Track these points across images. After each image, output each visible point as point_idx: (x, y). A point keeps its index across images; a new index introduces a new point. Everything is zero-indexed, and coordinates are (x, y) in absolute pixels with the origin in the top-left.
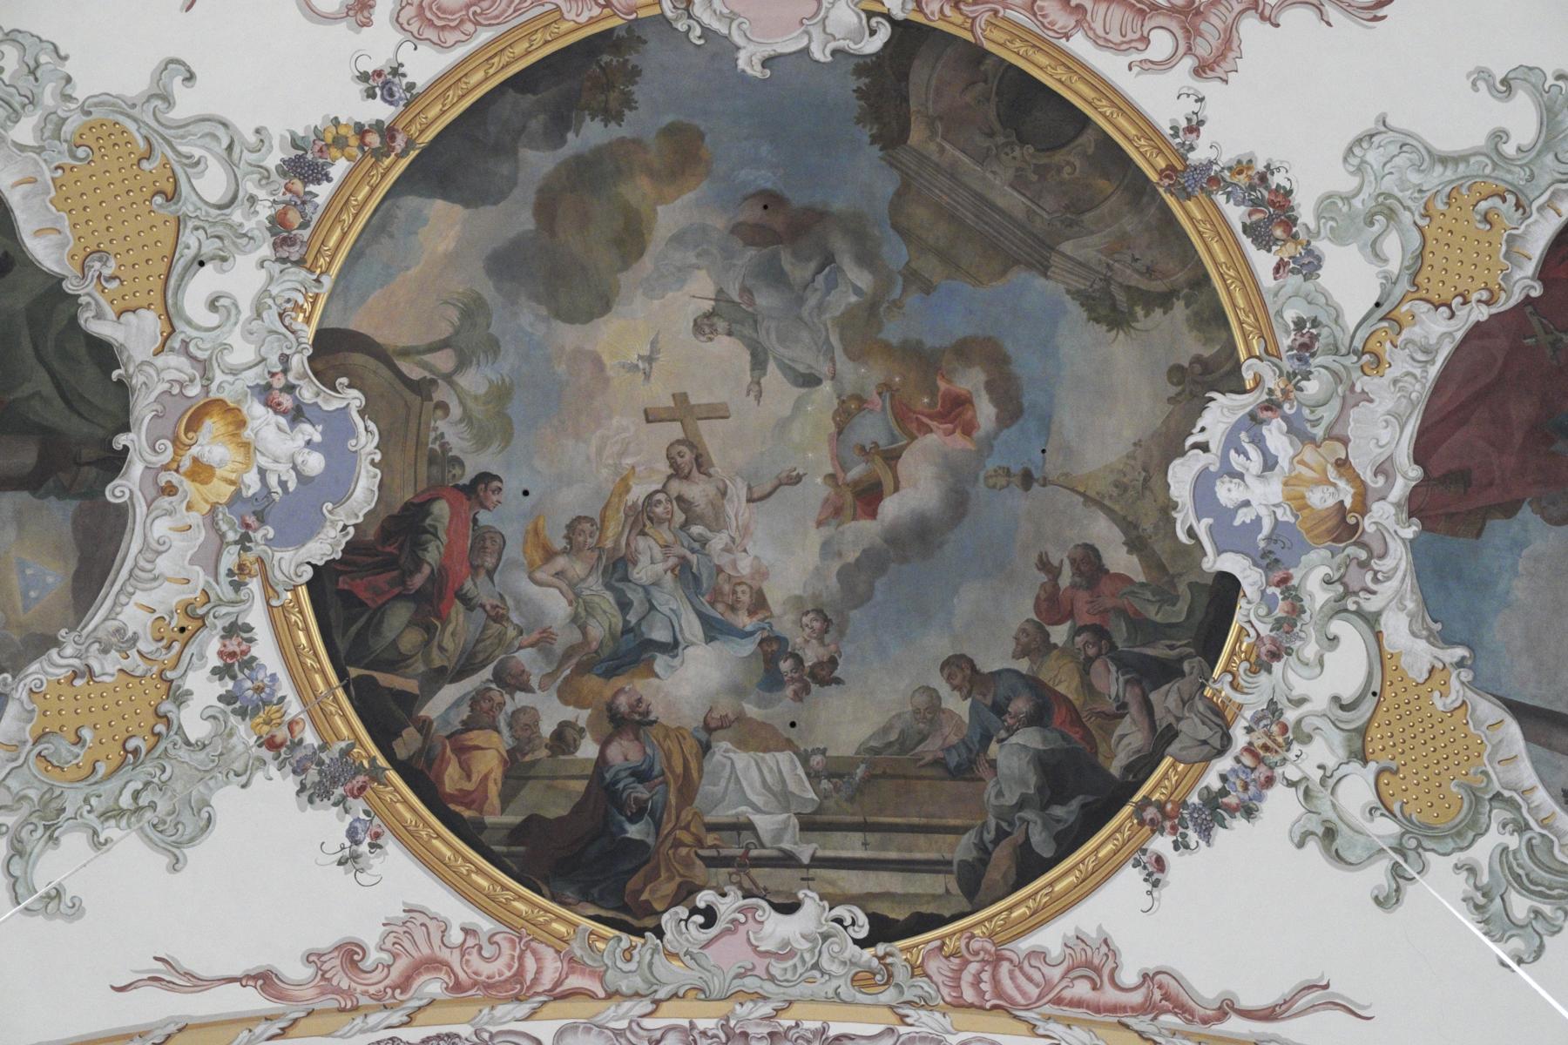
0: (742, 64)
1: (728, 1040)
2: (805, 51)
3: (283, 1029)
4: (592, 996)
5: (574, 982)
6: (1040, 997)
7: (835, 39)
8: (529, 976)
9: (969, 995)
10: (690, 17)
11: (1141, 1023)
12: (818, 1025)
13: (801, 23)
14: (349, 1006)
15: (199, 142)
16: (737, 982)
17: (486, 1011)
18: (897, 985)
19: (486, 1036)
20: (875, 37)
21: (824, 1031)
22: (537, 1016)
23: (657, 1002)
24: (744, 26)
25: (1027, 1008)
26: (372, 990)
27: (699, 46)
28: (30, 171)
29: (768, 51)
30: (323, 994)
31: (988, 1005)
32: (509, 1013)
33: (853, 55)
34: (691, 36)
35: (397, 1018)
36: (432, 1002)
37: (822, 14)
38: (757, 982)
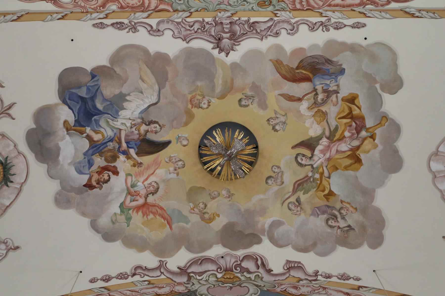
1: (216, 25)
3: (62, 16)
4: (168, 11)
5: (162, 7)
6: (323, 5)
8: (146, 5)
9: (298, 6)
11: (360, 9)
12: (246, 19)
14: (85, 11)
16: (218, 6)
17: (132, 15)
18: (273, 5)
19: (133, 23)
21: (249, 21)
22: (150, 17)
23: (191, 13)
25: (319, 9)
26: (92, 7)
30: (75, 7)
31: (305, 9)
32: (140, 16)
35: (102, 15)
36: (114, 12)
38: (225, 6)
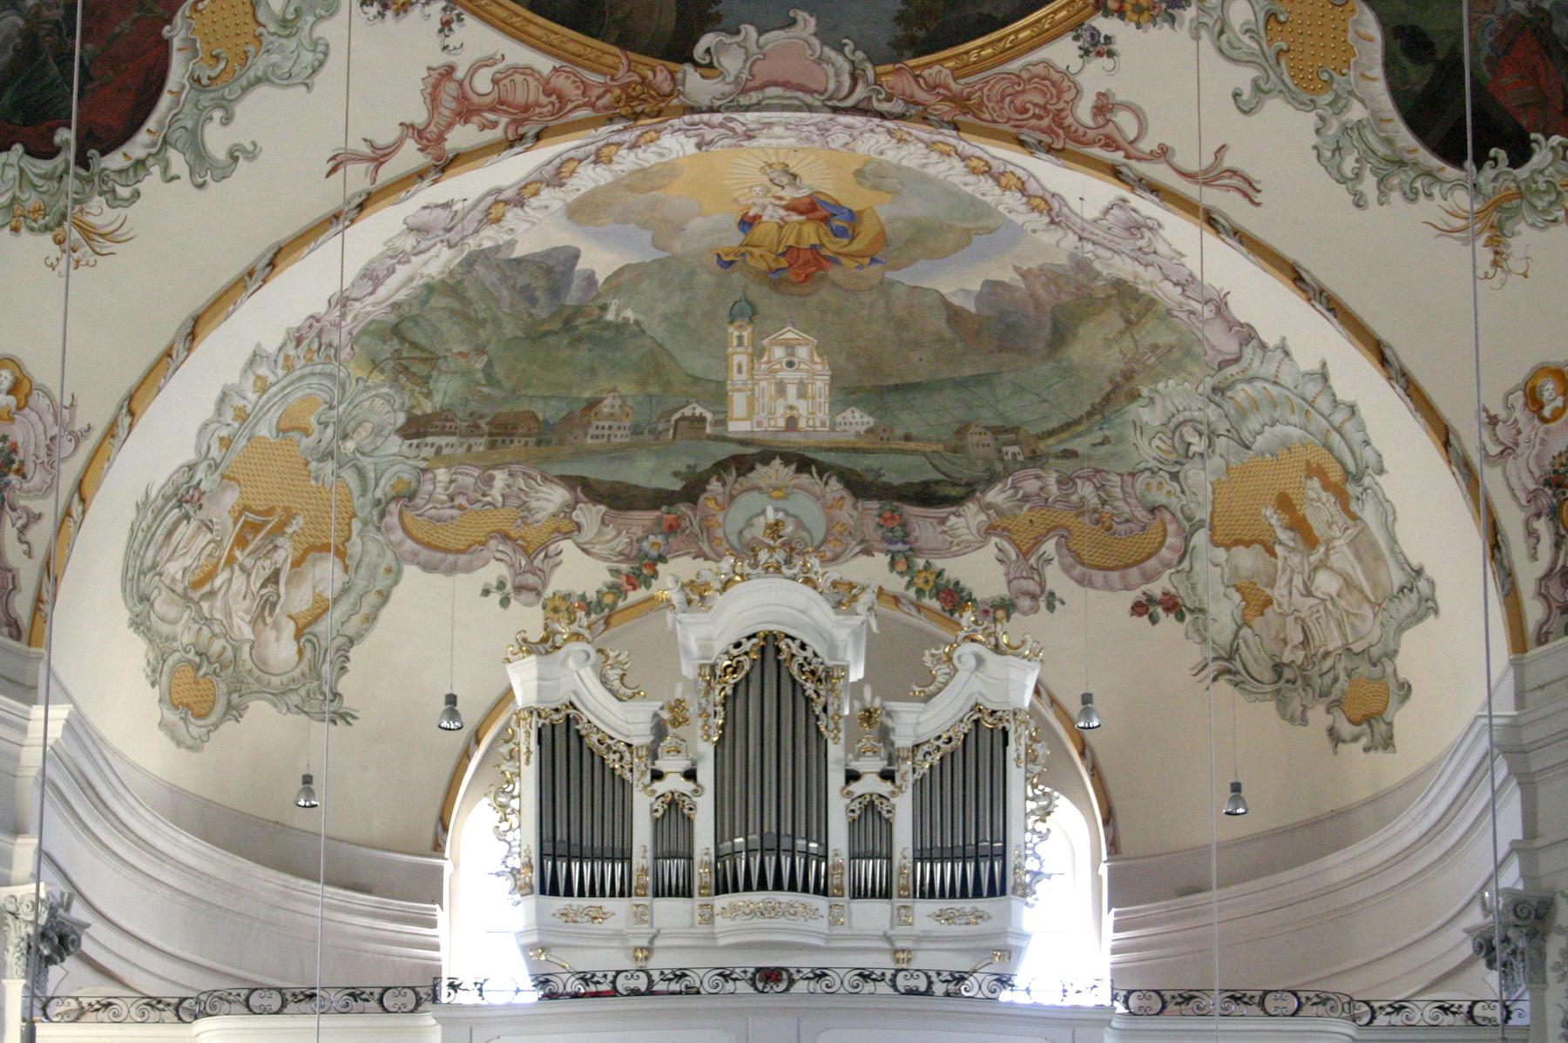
0: (812, 22)
2: (761, 32)
7: (738, 44)
10: (853, 62)
13: (764, 55)
15: (1241, 45)
20: (705, 47)
24: (810, 52)
27: (847, 38)
28: (1362, 83)
29: (793, 32)
33: (723, 30)
34: (852, 46)
37: (748, 65)
